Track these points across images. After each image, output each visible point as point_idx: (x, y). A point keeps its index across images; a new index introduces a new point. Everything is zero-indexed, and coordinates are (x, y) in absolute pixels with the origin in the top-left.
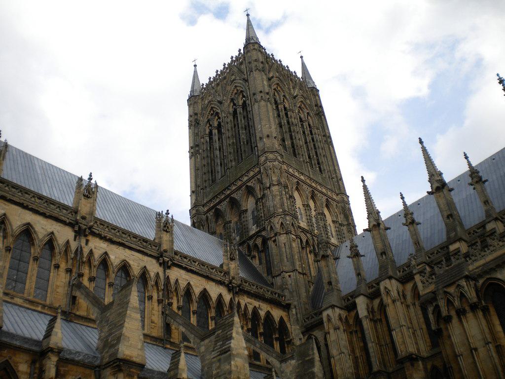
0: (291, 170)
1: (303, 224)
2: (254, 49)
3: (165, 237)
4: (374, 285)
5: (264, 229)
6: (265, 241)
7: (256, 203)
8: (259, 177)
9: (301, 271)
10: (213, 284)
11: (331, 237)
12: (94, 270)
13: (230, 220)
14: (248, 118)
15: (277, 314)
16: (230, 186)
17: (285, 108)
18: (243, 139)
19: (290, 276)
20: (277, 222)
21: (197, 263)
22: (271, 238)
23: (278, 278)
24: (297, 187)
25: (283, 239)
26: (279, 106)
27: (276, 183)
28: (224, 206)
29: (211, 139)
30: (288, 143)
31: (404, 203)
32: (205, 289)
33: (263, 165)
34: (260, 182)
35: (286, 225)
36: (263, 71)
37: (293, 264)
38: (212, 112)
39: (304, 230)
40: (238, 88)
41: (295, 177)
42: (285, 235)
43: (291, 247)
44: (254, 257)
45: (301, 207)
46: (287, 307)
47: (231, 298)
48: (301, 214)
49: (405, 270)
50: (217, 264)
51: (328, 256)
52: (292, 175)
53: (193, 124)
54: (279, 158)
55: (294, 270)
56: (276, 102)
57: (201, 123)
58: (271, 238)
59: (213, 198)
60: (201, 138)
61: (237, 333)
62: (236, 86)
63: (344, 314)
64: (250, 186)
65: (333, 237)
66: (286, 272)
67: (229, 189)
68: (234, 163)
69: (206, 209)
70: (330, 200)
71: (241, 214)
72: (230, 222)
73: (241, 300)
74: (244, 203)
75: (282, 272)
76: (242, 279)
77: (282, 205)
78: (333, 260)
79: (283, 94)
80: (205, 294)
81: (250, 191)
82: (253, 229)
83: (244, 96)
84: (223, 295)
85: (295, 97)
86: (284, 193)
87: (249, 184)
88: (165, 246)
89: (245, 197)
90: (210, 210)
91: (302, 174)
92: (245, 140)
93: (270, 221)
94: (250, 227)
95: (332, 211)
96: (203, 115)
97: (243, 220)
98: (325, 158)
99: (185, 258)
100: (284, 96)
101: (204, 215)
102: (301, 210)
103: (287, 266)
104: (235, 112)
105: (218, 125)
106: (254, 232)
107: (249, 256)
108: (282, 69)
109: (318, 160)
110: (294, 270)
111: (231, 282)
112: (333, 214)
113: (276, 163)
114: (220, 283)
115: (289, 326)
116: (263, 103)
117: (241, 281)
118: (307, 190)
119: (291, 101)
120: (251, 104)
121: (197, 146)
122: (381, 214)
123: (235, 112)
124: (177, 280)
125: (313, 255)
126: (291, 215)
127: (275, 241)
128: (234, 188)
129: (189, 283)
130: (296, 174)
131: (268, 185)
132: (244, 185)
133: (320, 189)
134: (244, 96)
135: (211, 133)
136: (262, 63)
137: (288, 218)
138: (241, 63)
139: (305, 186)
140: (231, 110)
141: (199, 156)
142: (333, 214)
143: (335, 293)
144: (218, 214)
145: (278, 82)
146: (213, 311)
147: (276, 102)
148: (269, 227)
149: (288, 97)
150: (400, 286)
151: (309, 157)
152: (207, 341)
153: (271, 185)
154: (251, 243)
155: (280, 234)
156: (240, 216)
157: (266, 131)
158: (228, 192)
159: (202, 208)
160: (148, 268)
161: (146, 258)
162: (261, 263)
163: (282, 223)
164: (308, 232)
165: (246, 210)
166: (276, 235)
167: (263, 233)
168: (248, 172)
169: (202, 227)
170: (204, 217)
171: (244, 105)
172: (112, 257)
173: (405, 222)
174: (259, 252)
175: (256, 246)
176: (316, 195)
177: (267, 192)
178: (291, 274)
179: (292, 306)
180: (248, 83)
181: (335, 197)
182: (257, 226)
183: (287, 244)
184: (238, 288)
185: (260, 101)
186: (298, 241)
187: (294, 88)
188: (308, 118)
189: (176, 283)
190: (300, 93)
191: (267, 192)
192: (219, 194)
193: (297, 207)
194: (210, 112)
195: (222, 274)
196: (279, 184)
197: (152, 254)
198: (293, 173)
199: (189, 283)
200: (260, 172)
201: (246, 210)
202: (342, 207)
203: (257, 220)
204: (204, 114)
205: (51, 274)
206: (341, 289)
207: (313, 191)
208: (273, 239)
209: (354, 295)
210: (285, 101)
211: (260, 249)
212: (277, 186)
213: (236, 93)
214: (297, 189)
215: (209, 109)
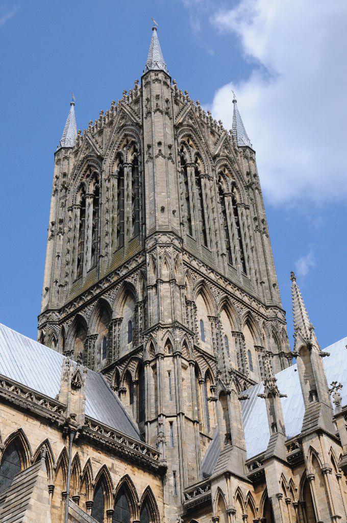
2: (157, 80)
7: (136, 310)
9: (190, 417)
10: (37, 423)
11: (249, 370)
13: (95, 333)
14: (138, 184)
16: (100, 282)
17: (197, 173)
18: (128, 213)
19: (171, 423)
20: (160, 337)
21: (12, 388)
22: (150, 362)
24: (201, 289)
25: (166, 364)
26: (188, 169)
27: (167, 280)
28: (89, 314)
29: (83, 213)
30: (196, 224)
32: (20, 430)
33: (149, 252)
34: (144, 276)
35: (175, 344)
36: (167, 113)
37: (178, 403)
38: (88, 173)
39: (204, 355)
41: (201, 274)
42: (171, 358)
43: (178, 379)
44: (124, 391)
45: (206, 320)
47: (65, 449)
48: (203, 330)
50: (51, 392)
51: (229, 393)
52: (196, 271)
53: (59, 189)
54: (176, 242)
55: (179, 414)
56: (183, 162)
57: (72, 189)
58: (150, 362)
60: (68, 211)
61: (40, 499)
64: (130, 283)
65: (252, 370)
66: (167, 417)
67: (99, 287)
68: (110, 248)
70: (253, 314)
71: (112, 324)
72: (96, 336)
73: (80, 454)
74: (118, 308)
75: (160, 416)
76: (88, 420)
77: (173, 312)
78: (237, 401)
79: (196, 151)
81: (129, 291)
82: (126, 348)
85: (214, 158)
86: (178, 295)
87: (128, 280)
89: (121, 299)
90: (69, 318)
91: (213, 271)
92: (131, 215)
93: (151, 335)
94: (122, 345)
95: (255, 330)
96: (75, 177)
98: (254, 252)
100: (198, 154)
101: (59, 325)
102: (205, 324)
103: (168, 407)
104: (121, 173)
105: (95, 192)
107: (116, 389)
108: (200, 114)
109: (242, 253)
110: (179, 414)
112: (257, 336)
113: (170, 250)
117: (86, 423)
118: (220, 296)
119: (209, 163)
121: (61, 221)
123: (121, 173)
126: (183, 328)
127: (154, 367)
128: (106, 285)
132: (121, 281)
133: (239, 296)
135: (83, 203)
136: (167, 101)
137: (177, 332)
139: (214, 289)
140: (116, 169)
141: (62, 237)
142: (257, 336)
144: (80, 326)
145: (191, 133)
147: (183, 162)
149: (203, 156)
151: (229, 249)
153: (159, 281)
154: (121, 369)
155: (164, 357)
156: (110, 329)
157: (161, 201)
158: (98, 291)
159: (58, 314)
163: (168, 340)
164: (211, 359)
165: (121, 320)
166: (157, 357)
168: (128, 262)
169: (53, 343)
171: (135, 161)
174: (131, 383)
175: (128, 374)
176: (231, 305)
177: (152, 292)
178: (174, 419)
180: (143, 130)
181: (262, 310)
182: (134, 344)
183: (172, 373)
184: (78, 433)
185: (157, 157)
186: (191, 370)
187: (215, 144)
188: (232, 190)
190: (224, 152)
191: (152, 292)
192: (83, 294)
193: (199, 319)
194: (85, 172)
196: (172, 281)
198: (198, 268)
200: (144, 262)
201: (121, 320)
202: (273, 327)
203: (133, 335)
204: (76, 175)
208: (152, 364)
210: (199, 161)
211: (134, 379)
212: (167, 284)
214: (201, 292)
215: (85, 168)
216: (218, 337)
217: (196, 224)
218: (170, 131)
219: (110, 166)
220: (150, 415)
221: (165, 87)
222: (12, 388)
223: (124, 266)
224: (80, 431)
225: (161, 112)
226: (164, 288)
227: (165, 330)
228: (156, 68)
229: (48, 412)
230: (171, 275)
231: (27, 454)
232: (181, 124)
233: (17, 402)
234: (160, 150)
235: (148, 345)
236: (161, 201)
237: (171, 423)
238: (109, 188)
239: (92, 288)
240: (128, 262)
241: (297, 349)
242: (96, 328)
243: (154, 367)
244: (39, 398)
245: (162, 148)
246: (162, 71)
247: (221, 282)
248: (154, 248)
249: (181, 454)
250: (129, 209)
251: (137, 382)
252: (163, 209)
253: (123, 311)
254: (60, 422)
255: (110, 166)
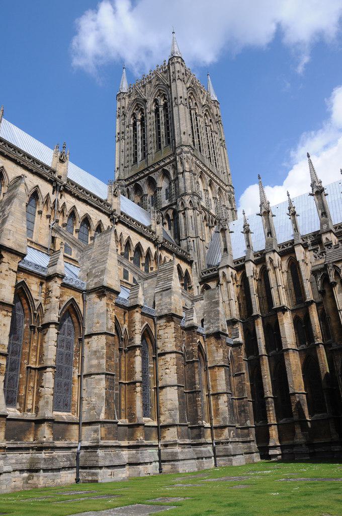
0: (198, 162)
1: (203, 203)
3: (115, 200)
4: (259, 255)
5: (176, 203)
6: (176, 213)
7: (170, 184)
8: (174, 163)
10: (145, 239)
12: (66, 218)
15: (184, 267)
17: (196, 113)
19: (193, 241)
20: (187, 199)
21: (135, 223)
23: (184, 241)
24: (201, 176)
28: (143, 183)
31: (289, 198)
34: (175, 168)
37: (196, 232)
39: (204, 209)
40: (161, 92)
43: (196, 220)
44: (165, 224)
45: (203, 191)
46: (190, 263)
49: (284, 247)
52: (199, 166)
54: (191, 151)
55: (197, 237)
59: (134, 175)
62: (159, 90)
63: (234, 272)
69: (127, 183)
75: (188, 237)
80: (139, 247)
81: (166, 174)
82: (165, 203)
83: (166, 99)
84: (151, 248)
87: (165, 168)
88: (114, 207)
89: (161, 178)
91: (205, 166)
92: (164, 134)
94: (163, 201)
97: (158, 195)
99: (128, 217)
100: (196, 103)
103: (191, 233)
106: (166, 205)
110: (197, 237)
111: (156, 240)
113: (189, 155)
114: (149, 239)
115: (191, 276)
116: (182, 105)
120: (172, 106)
122: (270, 204)
124: (121, 233)
125: (208, 227)
127: (184, 214)
128: (152, 169)
129: (129, 237)
130: (201, 165)
131: (181, 171)
134: (165, 99)
137: (195, 197)
138: (165, 72)
139: (206, 176)
140: (154, 108)
143: (229, 256)
144: (138, 189)
146: (144, 259)
148: (180, 204)
150: (280, 258)
152: (149, 280)
153: (184, 171)
157: (183, 129)
158: (147, 172)
160: (103, 221)
161: (101, 214)
162: (170, 229)
163: (190, 201)
165: (161, 188)
166: (185, 209)
167: (174, 207)
168: (165, 159)
170: (125, 189)
171: (165, 105)
172: (79, 210)
173: (288, 213)
175: (167, 216)
177: (180, 176)
179: (194, 263)
182: (169, 201)
183: (193, 218)
189: (120, 236)
195: (151, 233)
196: (190, 171)
197: (106, 211)
199: (129, 237)
200: (175, 160)
201: (161, 188)
205: (36, 218)
206: (233, 255)
207: (211, 180)
208: (183, 212)
209: (244, 260)
213: (159, 95)
214: (201, 177)
216: (208, 200)
217: (196, 140)
218: (185, 91)
219: (150, 106)
220: (183, 236)
221: (181, 66)
222: (135, 223)
223: (162, 160)
224: (161, 243)
225: (181, 80)
226: (187, 174)
227: (189, 196)
228: (177, 55)
229: (149, 235)
230: (190, 168)
231: (143, 253)
232: (190, 87)
233: (137, 230)
234: (181, 101)
235: (181, 202)
236: (183, 129)
237: (193, 241)
238: (151, 119)
239: (144, 170)
240: (165, 159)
241: (262, 213)
242: (147, 190)
243: (184, 214)
244: (145, 228)
245: (182, 99)
246: (180, 57)
247: (208, 172)
248: (181, 153)
249: (199, 255)
250: (163, 130)
251: (172, 220)
252: (184, 133)
253: (162, 183)
254: (154, 240)
255: (150, 106)
